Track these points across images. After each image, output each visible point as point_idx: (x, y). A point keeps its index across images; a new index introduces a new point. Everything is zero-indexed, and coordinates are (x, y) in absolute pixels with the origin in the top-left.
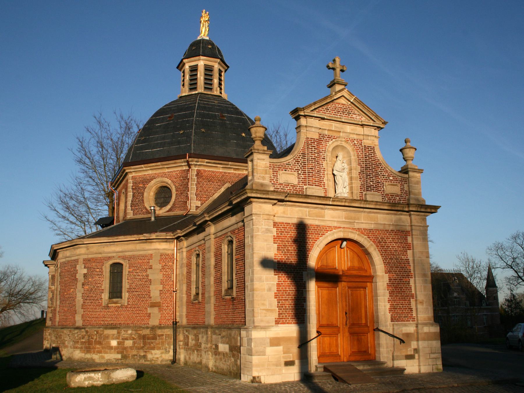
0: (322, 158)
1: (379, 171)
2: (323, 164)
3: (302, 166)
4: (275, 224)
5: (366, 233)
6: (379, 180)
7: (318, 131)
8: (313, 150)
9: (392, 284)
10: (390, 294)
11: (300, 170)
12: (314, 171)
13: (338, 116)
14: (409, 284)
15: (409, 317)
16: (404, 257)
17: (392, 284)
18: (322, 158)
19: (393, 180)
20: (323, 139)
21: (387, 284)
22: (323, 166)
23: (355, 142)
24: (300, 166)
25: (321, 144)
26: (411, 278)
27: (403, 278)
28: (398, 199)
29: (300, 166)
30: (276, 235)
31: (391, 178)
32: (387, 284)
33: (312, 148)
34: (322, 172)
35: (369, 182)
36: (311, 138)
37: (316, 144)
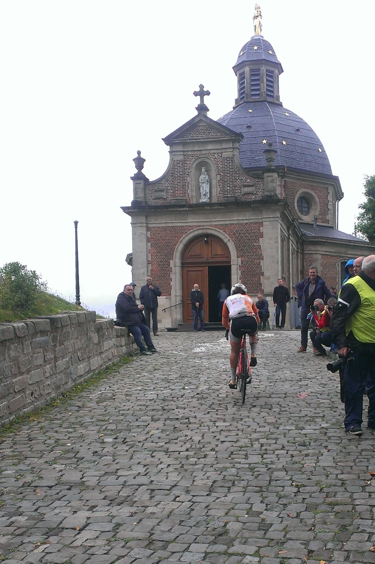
0: (187, 174)
1: (237, 177)
2: (187, 179)
3: (171, 183)
4: (148, 229)
5: (223, 228)
6: (237, 184)
7: (182, 153)
8: (179, 169)
9: (244, 265)
10: (241, 273)
11: (169, 187)
12: (179, 186)
13: (200, 137)
14: (260, 264)
15: (258, 290)
16: (256, 244)
17: (244, 265)
18: (187, 174)
19: (250, 182)
20: (188, 159)
21: (240, 265)
22: (187, 181)
23: (216, 156)
24: (169, 183)
25: (186, 163)
26: (261, 260)
27: (254, 260)
28: (254, 197)
29: (169, 183)
30: (150, 237)
31: (248, 181)
32: (240, 265)
33: (178, 168)
34: (187, 185)
35: (226, 187)
36: (177, 160)
37: (181, 164)
